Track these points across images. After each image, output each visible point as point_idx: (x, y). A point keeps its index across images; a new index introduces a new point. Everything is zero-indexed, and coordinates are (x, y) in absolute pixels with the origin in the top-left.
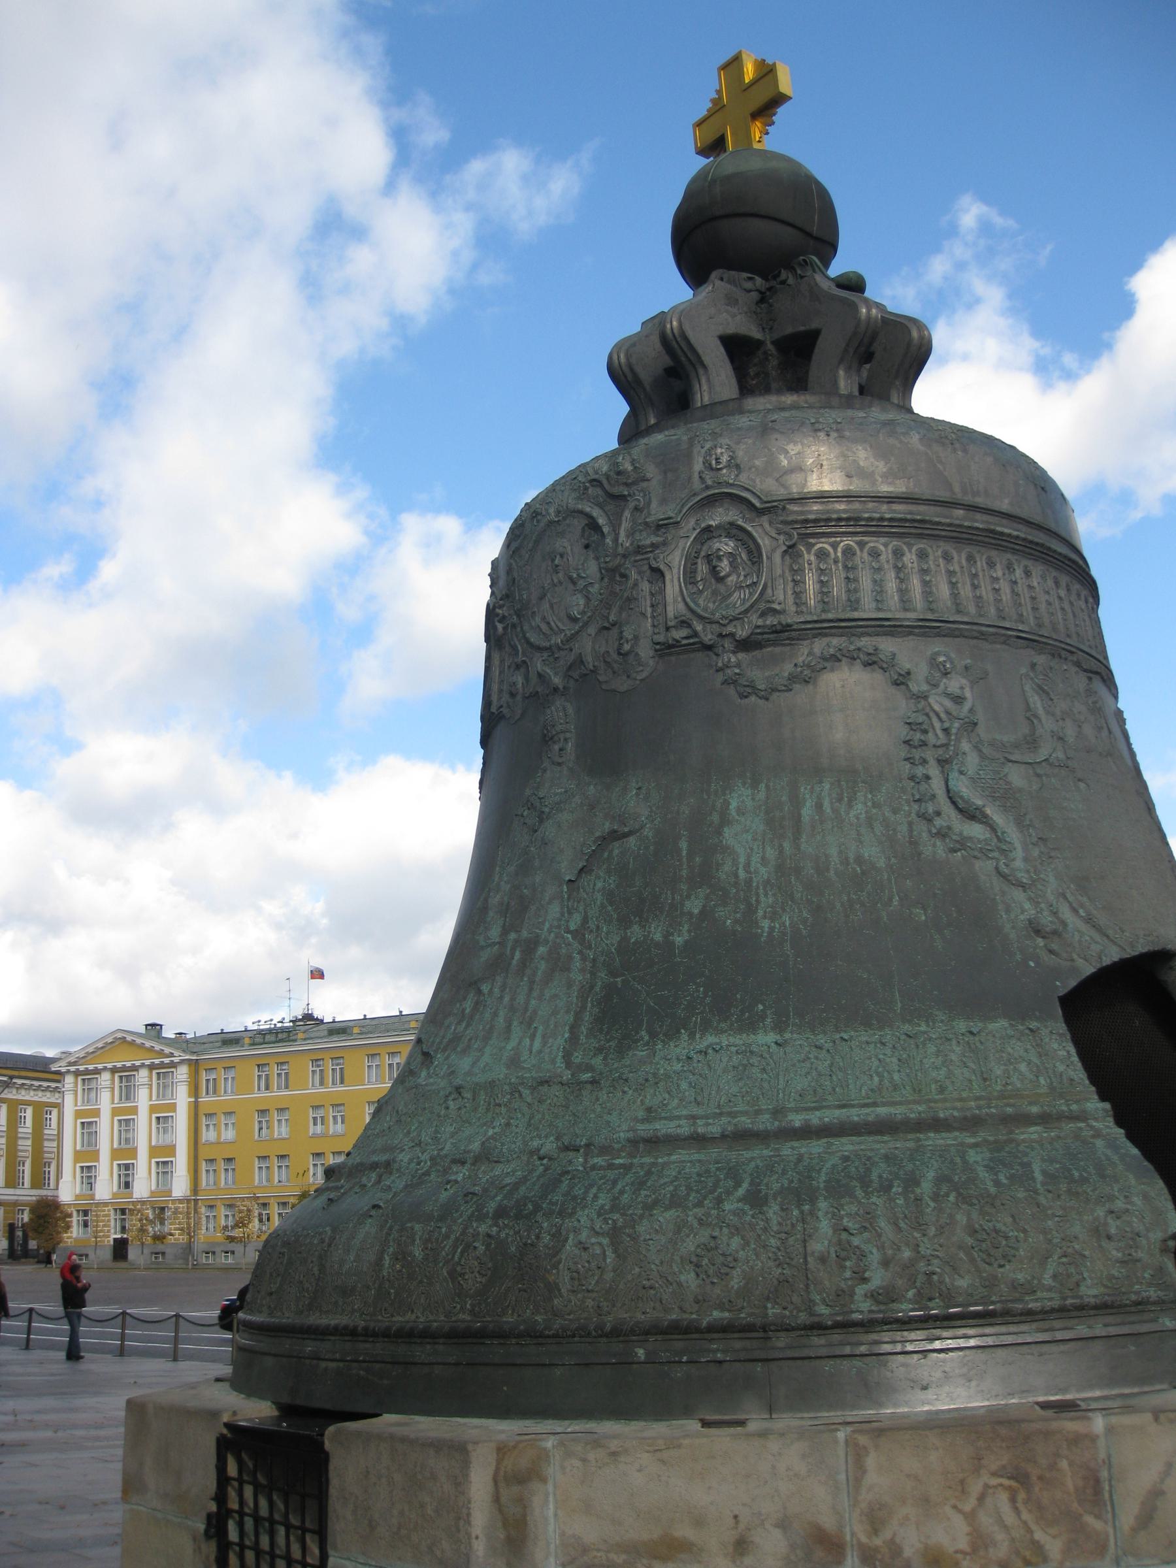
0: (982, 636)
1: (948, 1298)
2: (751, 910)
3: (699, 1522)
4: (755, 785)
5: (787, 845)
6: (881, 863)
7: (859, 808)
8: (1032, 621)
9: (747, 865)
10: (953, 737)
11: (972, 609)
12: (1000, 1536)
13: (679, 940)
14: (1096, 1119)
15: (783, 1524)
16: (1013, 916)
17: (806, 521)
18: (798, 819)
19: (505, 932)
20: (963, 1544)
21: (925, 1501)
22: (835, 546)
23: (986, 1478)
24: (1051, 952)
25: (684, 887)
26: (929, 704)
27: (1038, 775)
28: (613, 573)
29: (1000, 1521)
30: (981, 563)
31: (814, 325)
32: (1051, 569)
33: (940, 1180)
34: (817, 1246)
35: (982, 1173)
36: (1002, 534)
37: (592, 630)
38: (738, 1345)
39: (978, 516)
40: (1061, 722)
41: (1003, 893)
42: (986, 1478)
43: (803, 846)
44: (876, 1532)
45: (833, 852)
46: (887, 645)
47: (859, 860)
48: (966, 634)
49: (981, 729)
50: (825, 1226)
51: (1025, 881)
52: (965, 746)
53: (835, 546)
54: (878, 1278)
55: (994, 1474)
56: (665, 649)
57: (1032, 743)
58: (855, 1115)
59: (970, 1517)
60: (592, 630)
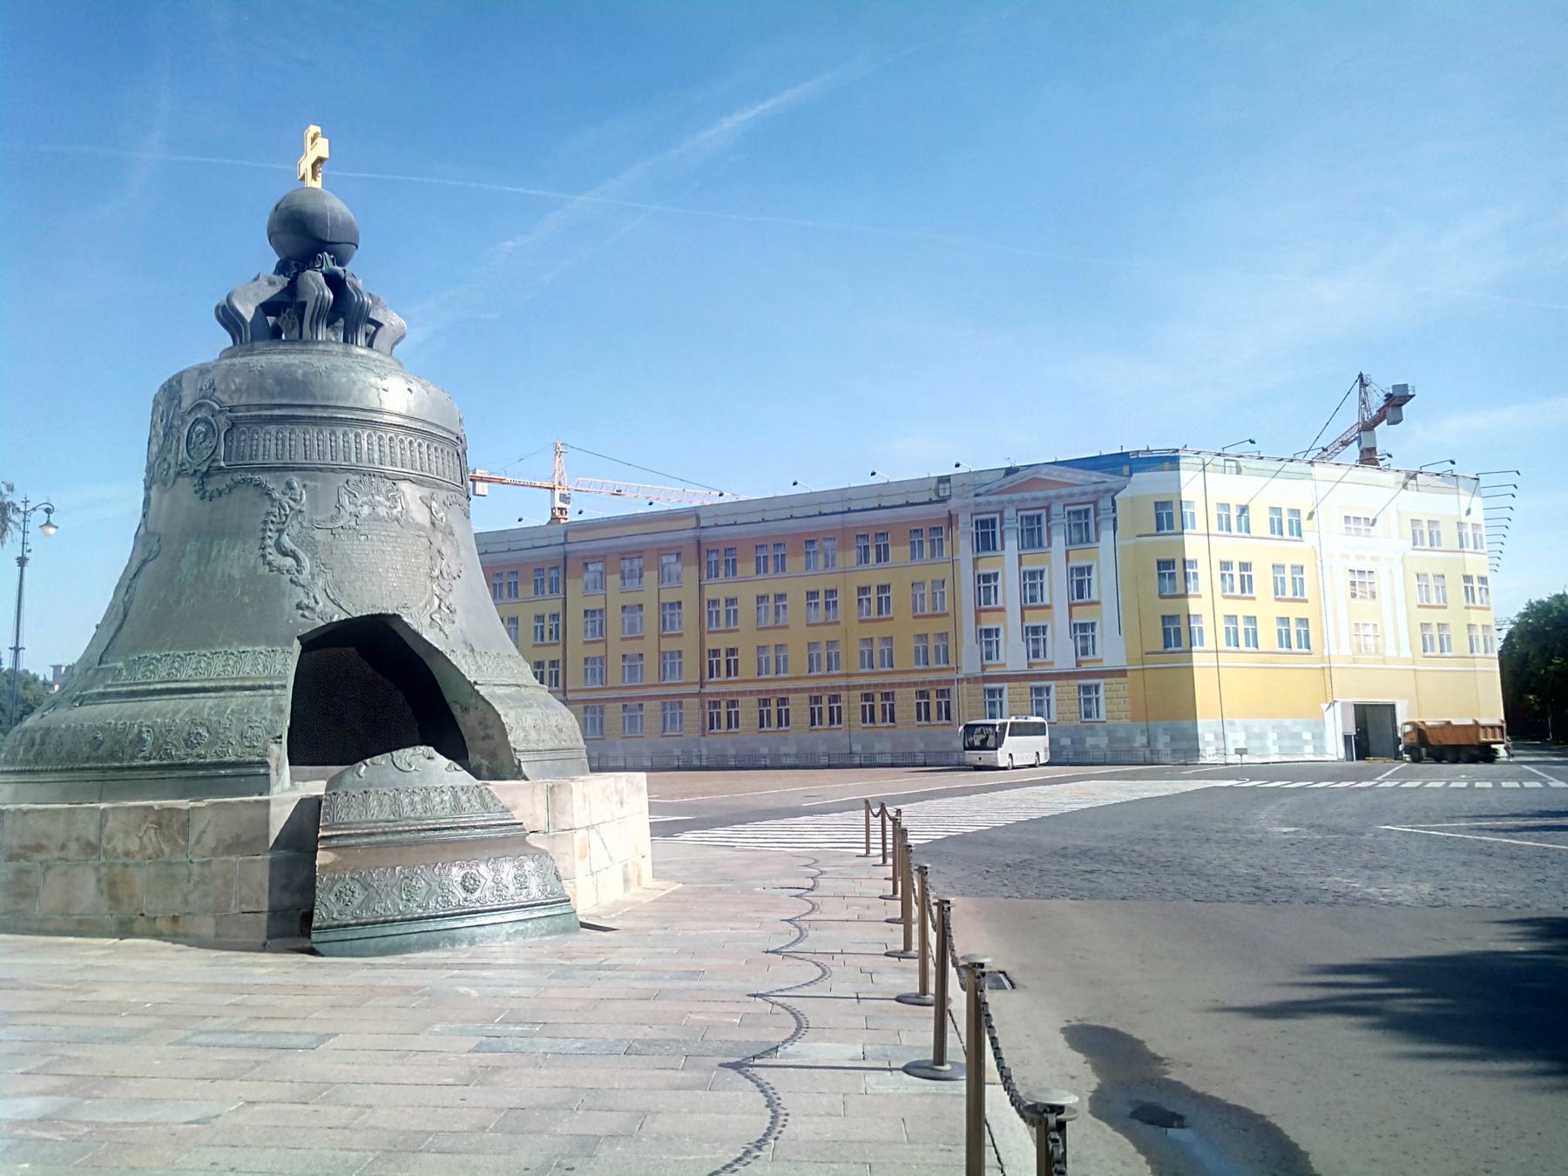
0: (320, 470)
1: (170, 756)
3: (49, 838)
5: (202, 568)
6: (237, 577)
7: (236, 551)
8: (353, 460)
12: (149, 846)
15: (77, 840)
17: (237, 417)
20: (137, 849)
21: (127, 833)
22: (249, 429)
23: (148, 824)
24: (303, 616)
30: (326, 433)
33: (190, 712)
35: (206, 710)
39: (330, 410)
41: (291, 590)
42: (148, 824)
44: (109, 843)
45: (220, 571)
46: (263, 478)
47: (229, 575)
50: (136, 730)
52: (295, 522)
53: (249, 429)
55: (152, 823)
56: (178, 474)
57: (332, 519)
59: (141, 838)
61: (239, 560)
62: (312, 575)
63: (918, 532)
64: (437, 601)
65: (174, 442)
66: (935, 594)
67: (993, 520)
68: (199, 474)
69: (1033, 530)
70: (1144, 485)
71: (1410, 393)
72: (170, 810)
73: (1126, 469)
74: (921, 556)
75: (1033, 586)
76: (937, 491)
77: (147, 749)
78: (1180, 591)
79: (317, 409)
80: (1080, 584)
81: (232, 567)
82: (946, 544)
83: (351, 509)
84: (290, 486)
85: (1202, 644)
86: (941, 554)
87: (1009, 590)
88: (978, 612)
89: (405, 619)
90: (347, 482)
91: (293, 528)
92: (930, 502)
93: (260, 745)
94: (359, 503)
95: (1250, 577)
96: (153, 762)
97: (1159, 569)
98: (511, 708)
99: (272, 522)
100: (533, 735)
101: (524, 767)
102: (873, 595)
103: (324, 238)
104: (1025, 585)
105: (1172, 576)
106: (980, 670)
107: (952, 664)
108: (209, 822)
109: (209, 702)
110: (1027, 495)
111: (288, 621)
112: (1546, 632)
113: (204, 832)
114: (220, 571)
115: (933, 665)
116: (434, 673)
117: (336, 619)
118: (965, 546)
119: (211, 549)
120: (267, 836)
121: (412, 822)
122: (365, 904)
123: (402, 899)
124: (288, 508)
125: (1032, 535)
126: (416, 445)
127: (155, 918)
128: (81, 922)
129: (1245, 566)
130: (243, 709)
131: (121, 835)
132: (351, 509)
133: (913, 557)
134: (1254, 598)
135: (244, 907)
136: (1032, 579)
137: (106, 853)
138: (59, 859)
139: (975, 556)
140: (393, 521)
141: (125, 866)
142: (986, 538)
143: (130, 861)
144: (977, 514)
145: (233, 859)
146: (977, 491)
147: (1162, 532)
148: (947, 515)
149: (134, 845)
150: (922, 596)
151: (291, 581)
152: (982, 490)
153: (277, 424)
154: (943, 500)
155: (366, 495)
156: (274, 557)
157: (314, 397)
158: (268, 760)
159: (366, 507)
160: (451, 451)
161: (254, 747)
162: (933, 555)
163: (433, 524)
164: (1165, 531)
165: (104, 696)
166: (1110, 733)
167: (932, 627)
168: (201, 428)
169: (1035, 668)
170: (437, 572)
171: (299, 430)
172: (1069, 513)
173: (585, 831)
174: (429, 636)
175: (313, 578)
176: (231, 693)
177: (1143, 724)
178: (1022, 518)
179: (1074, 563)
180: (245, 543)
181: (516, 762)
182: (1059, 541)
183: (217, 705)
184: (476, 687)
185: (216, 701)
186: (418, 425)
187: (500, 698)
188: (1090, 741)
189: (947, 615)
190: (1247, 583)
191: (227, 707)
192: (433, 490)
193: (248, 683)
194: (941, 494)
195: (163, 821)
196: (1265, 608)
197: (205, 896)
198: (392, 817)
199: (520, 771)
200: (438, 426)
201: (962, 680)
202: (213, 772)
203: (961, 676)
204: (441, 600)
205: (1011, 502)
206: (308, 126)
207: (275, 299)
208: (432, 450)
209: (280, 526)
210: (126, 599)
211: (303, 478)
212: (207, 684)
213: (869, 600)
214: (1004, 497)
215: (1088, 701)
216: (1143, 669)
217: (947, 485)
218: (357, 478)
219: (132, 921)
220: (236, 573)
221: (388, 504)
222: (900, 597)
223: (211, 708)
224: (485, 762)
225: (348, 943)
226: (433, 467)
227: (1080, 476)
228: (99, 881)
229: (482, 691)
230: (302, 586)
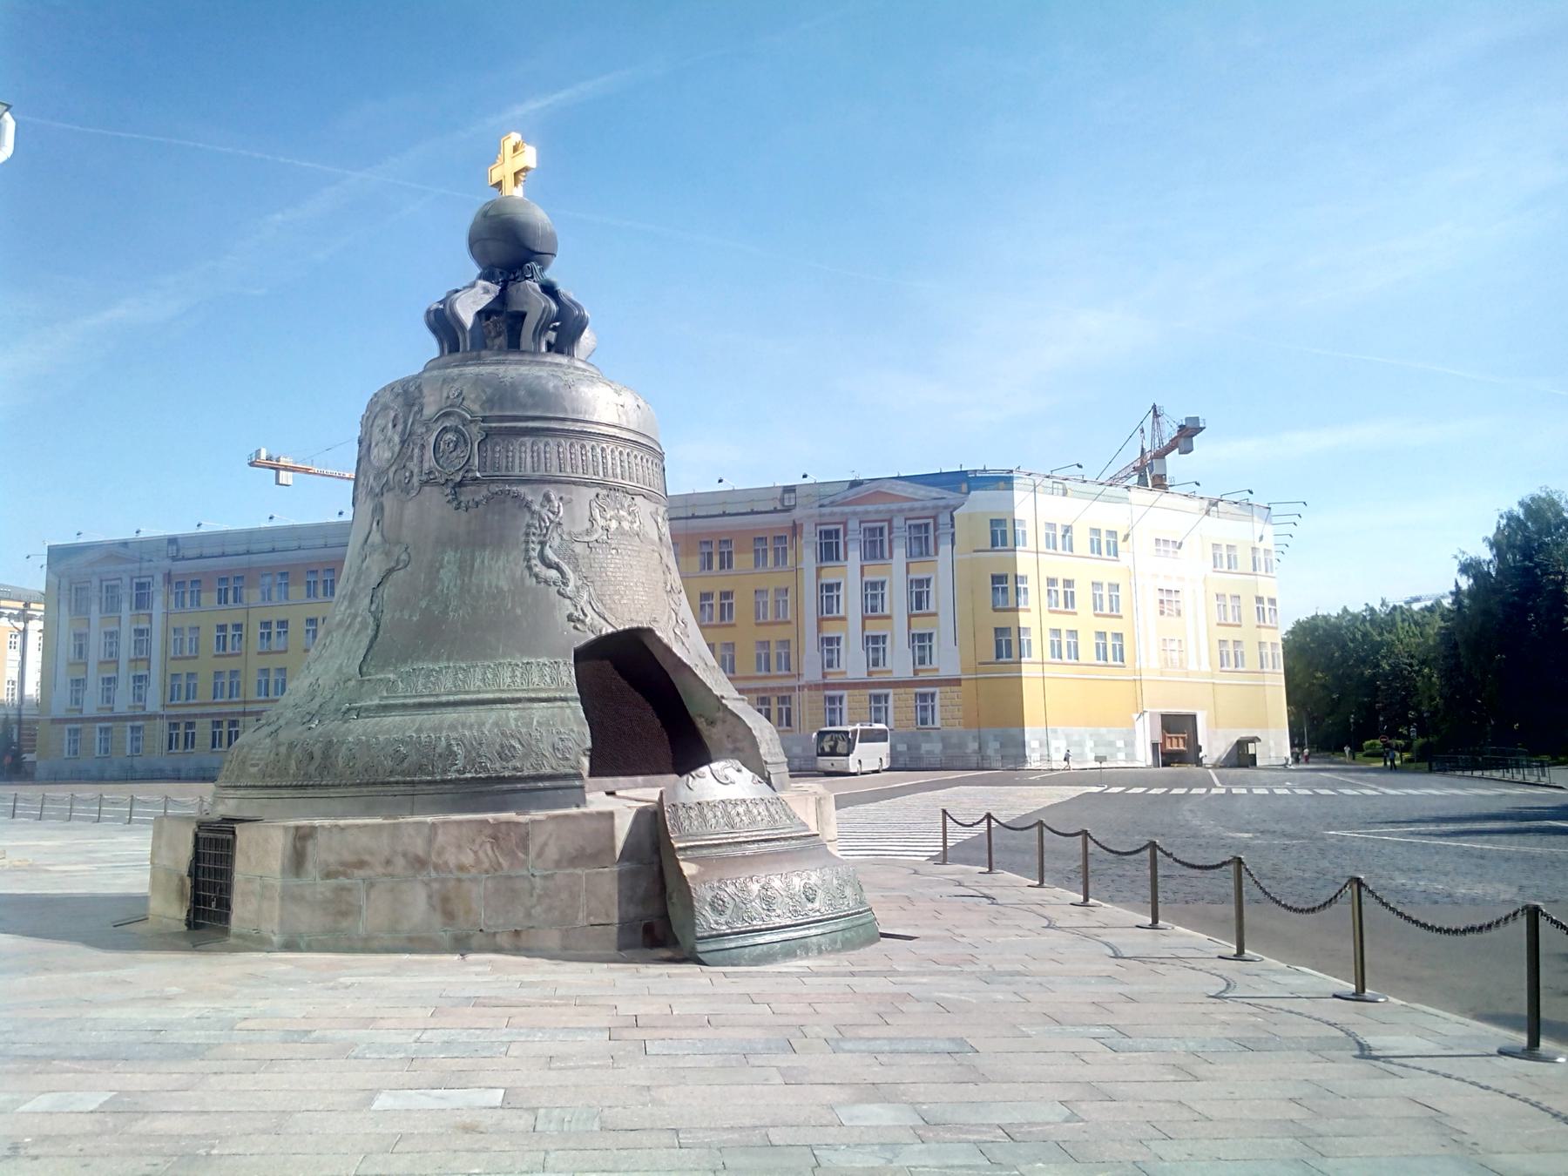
0: (574, 483)
2: (447, 607)
3: (372, 853)
4: (456, 552)
5: (466, 579)
6: (506, 589)
7: (501, 563)
8: (601, 473)
9: (448, 588)
11: (569, 469)
12: (486, 860)
13: (415, 619)
15: (405, 855)
17: (491, 427)
18: (473, 566)
19: (346, 610)
20: (472, 863)
21: (459, 847)
24: (575, 628)
25: (420, 595)
28: (403, 442)
29: (487, 855)
31: (525, 309)
33: (496, 724)
34: (438, 750)
35: (513, 722)
37: (393, 469)
38: (402, 788)
39: (579, 424)
41: (560, 601)
43: (473, 579)
45: (486, 583)
46: (523, 490)
47: (497, 587)
49: (565, 528)
50: (444, 743)
52: (555, 535)
54: (460, 763)
56: (424, 483)
57: (588, 532)
58: (468, 697)
59: (475, 853)
60: (393, 469)
61: (504, 571)
62: (577, 588)
63: (763, 540)
65: (416, 451)
66: (777, 602)
67: (837, 531)
68: (451, 484)
69: (875, 541)
70: (980, 502)
71: (1201, 425)
72: (508, 823)
73: (964, 487)
74: (765, 564)
75: (874, 597)
76: (782, 500)
77: (460, 763)
78: (1012, 604)
79: (569, 423)
80: (919, 595)
81: (498, 578)
82: (790, 553)
83: (601, 522)
84: (547, 498)
85: (1030, 656)
86: (785, 562)
87: (851, 602)
88: (820, 621)
91: (556, 542)
92: (775, 511)
93: (571, 757)
94: (608, 517)
95: (1072, 593)
96: (469, 775)
97: (993, 583)
99: (534, 534)
102: (716, 601)
104: (866, 596)
105: (1005, 590)
106: (820, 677)
107: (794, 670)
108: (551, 835)
109: (512, 713)
110: (870, 508)
112: (1311, 648)
113: (545, 844)
114: (486, 583)
115: (774, 671)
116: (677, 687)
117: (604, 633)
118: (809, 557)
119: (473, 559)
120: (613, 849)
125: (875, 547)
127: (495, 934)
128: (410, 939)
129: (1068, 583)
133: (756, 565)
134: (1075, 613)
135: (592, 920)
136: (873, 590)
137: (436, 867)
138: (385, 875)
139: (819, 565)
141: (459, 880)
142: (830, 549)
143: (463, 876)
144: (821, 524)
145: (579, 871)
146: (822, 502)
147: (996, 548)
148: (791, 525)
149: (468, 858)
150: (765, 604)
152: (826, 501)
153: (531, 436)
154: (788, 509)
156: (539, 568)
157: (565, 411)
159: (614, 521)
162: (776, 563)
163: (660, 539)
164: (999, 548)
165: (386, 708)
166: (944, 740)
167: (775, 634)
168: (450, 436)
169: (874, 676)
170: (669, 588)
172: (910, 527)
174: (678, 650)
175: (578, 592)
176: (528, 705)
177: (974, 731)
178: (865, 530)
179: (914, 576)
180: (508, 555)
182: (900, 553)
184: (724, 701)
185: (517, 713)
188: (925, 747)
189: (789, 623)
190: (1070, 599)
193: (543, 695)
194: (786, 504)
195: (500, 835)
196: (1085, 622)
197: (550, 909)
201: (804, 687)
202: (532, 785)
203: (802, 682)
205: (855, 513)
206: (509, 132)
207: (491, 307)
209: (541, 538)
210: (373, 608)
211: (559, 491)
212: (504, 696)
213: (711, 606)
214: (847, 509)
215: (924, 709)
216: (976, 679)
217: (793, 495)
218: (605, 492)
219: (468, 937)
220: (504, 585)
221: (630, 518)
222: (742, 604)
223: (516, 720)
225: (727, 952)
227: (922, 492)
228: (430, 897)
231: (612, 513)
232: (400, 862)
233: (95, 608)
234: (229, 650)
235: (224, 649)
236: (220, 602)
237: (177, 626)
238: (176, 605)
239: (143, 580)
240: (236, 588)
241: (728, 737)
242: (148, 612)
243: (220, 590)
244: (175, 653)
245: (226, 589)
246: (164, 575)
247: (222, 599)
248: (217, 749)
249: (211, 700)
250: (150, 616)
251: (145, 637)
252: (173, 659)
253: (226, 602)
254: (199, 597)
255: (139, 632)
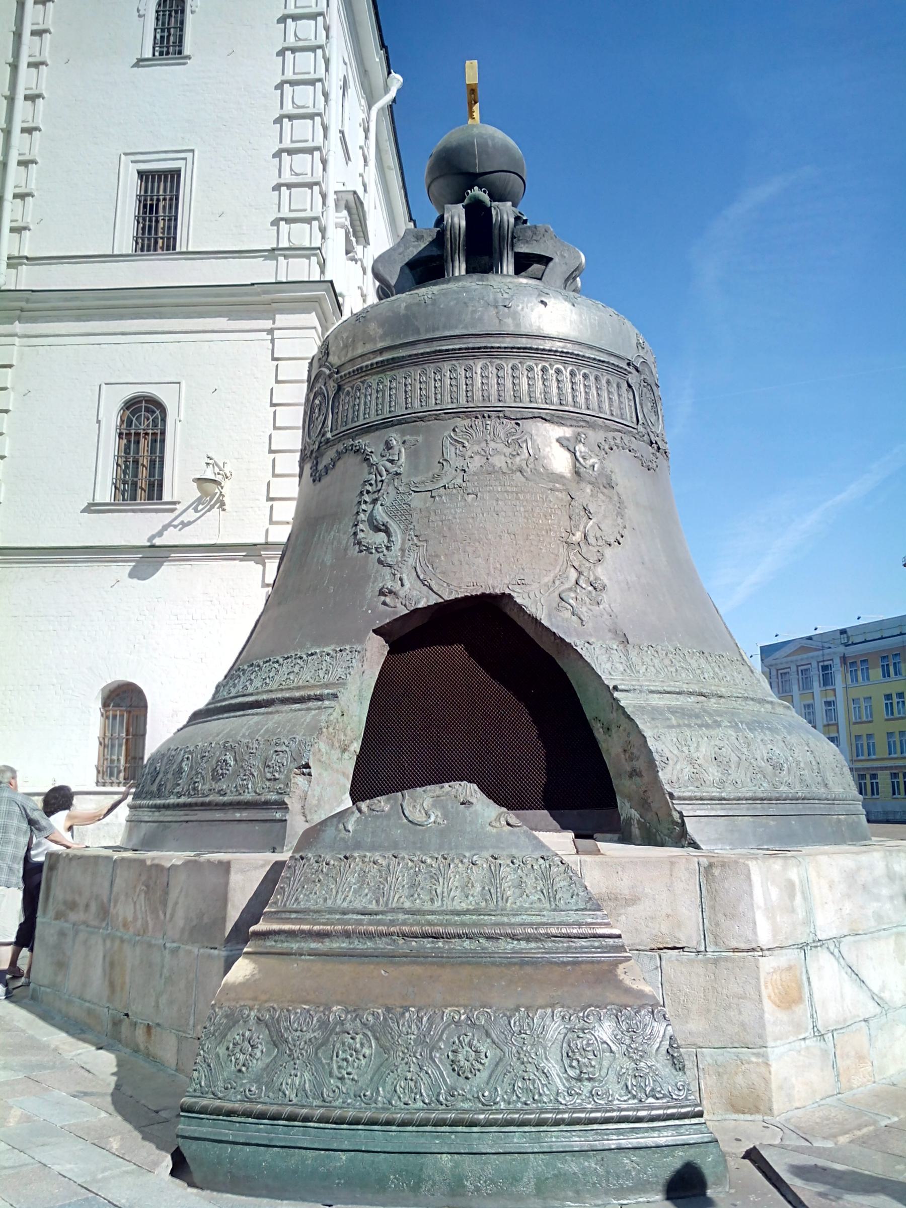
0: (421, 419)
7: (333, 533)
8: (463, 401)
10: (385, 484)
14: (328, 699)
16: (376, 584)
24: (384, 603)
26: (377, 469)
27: (432, 497)
32: (494, 360)
35: (244, 730)
36: (447, 350)
40: (468, 460)
48: (409, 420)
51: (391, 563)
52: (391, 489)
59: (135, 903)
62: (402, 550)
64: (573, 575)
81: (326, 553)
84: (388, 446)
89: (519, 600)
90: (454, 430)
91: (389, 496)
93: (282, 777)
94: (469, 453)
98: (671, 727)
99: (368, 492)
100: (713, 773)
101: (691, 826)
103: (472, 171)
111: (367, 611)
120: (224, 919)
121: (401, 917)
122: (266, 1078)
123: (331, 1075)
124: (384, 473)
126: (552, 372)
130: (277, 728)
131: (122, 898)
132: (460, 463)
140: (513, 472)
141: (122, 941)
151: (380, 562)
155: (479, 442)
158: (287, 800)
159: (477, 458)
160: (614, 380)
161: (275, 779)
170: (578, 536)
171: (400, 373)
173: (794, 955)
180: (340, 523)
181: (676, 816)
183: (257, 723)
184: (616, 694)
186: (569, 348)
187: (655, 713)
191: (263, 725)
192: (580, 430)
193: (297, 694)
198: (373, 906)
199: (684, 833)
200: (591, 347)
204: (580, 573)
208: (579, 378)
209: (376, 496)
211: (403, 434)
218: (467, 422)
221: (508, 451)
224: (635, 814)
225: (229, 1148)
226: (581, 399)
229: (625, 700)
230: (390, 566)
231: (476, 448)
232: (93, 908)
233: (795, 688)
234: (896, 714)
235: (892, 714)
236: (884, 676)
237: (855, 697)
238: (852, 681)
239: (826, 663)
240: (895, 664)
241: (625, 751)
242: (832, 687)
243: (883, 666)
244: (856, 718)
245: (888, 665)
246: (840, 657)
247: (886, 674)
248: (896, 796)
249: (887, 756)
250: (834, 690)
251: (832, 707)
252: (855, 723)
253: (889, 676)
254: (868, 673)
255: (828, 703)
